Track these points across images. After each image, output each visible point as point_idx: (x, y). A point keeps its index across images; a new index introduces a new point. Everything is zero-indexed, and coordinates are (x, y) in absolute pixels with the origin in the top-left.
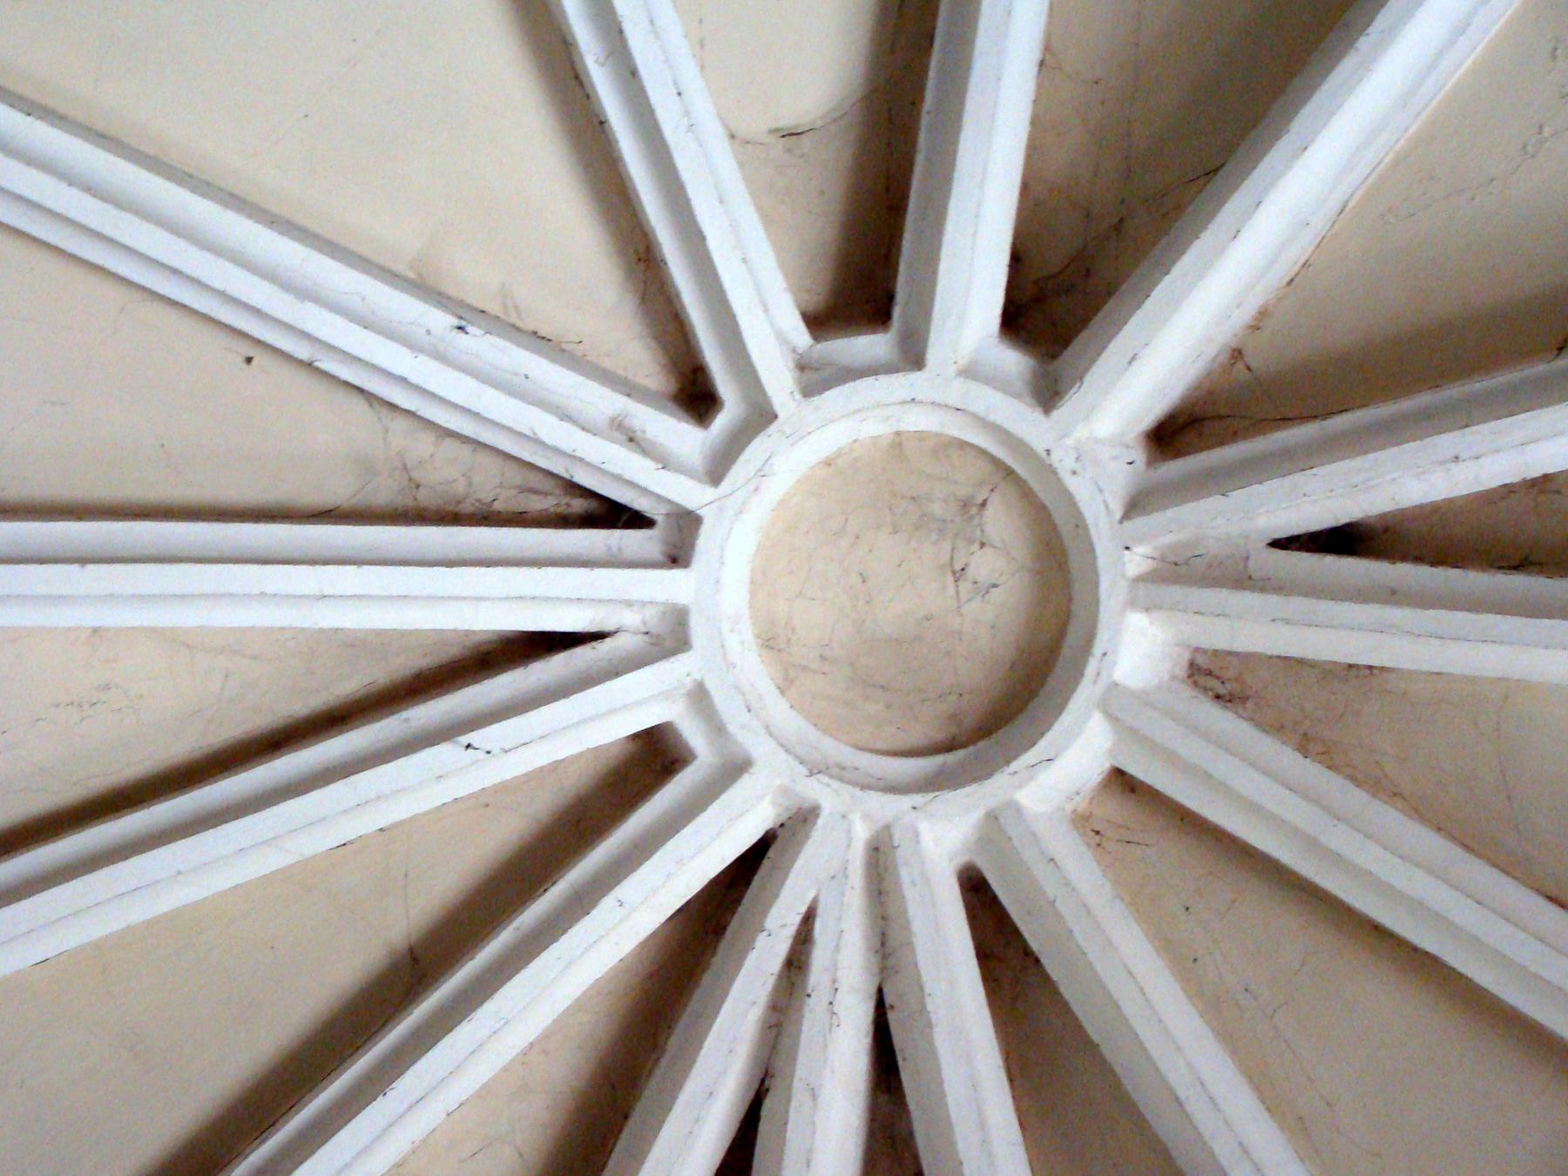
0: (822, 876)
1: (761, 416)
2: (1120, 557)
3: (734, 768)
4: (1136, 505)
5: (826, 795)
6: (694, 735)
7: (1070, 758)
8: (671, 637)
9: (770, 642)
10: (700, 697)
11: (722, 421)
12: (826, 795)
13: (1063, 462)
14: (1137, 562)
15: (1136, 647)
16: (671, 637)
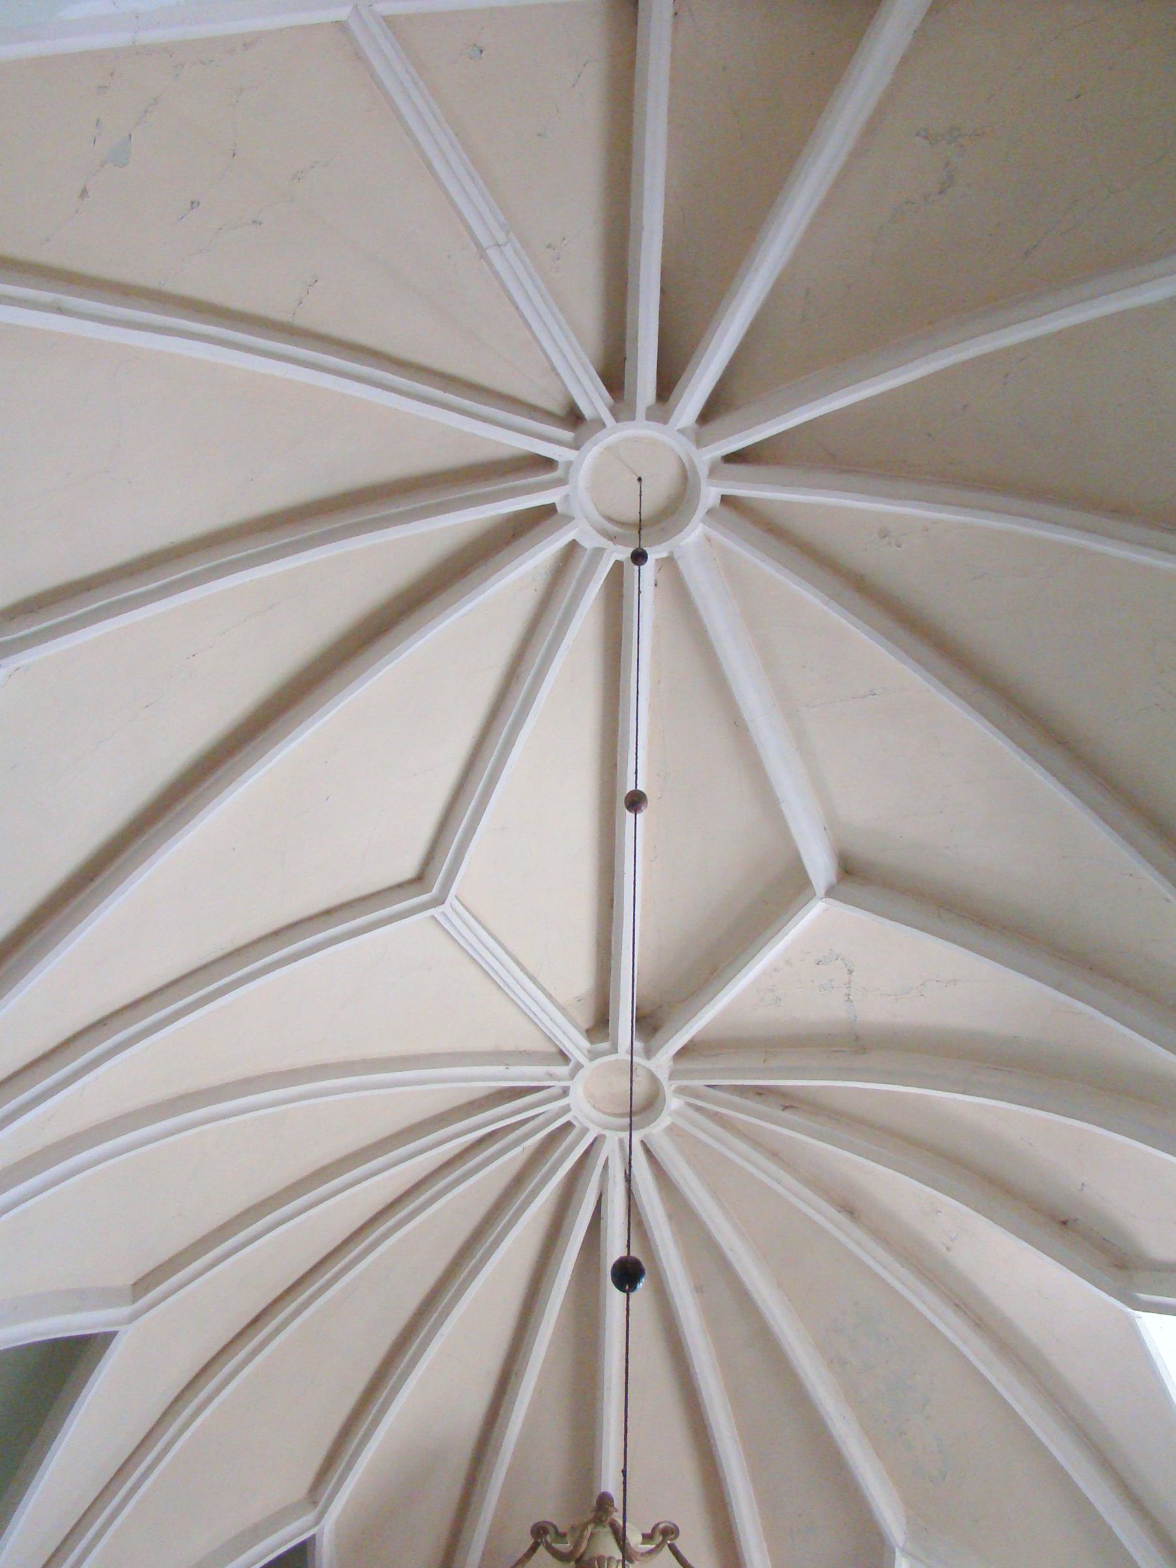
0: (611, 1150)
1: (579, 1066)
2: (668, 1087)
3: (585, 1131)
4: (672, 1076)
5: (606, 1133)
6: (575, 1123)
7: (665, 1120)
8: (567, 1109)
9: (590, 1097)
10: (575, 1117)
11: (571, 1064)
12: (606, 1133)
13: (653, 1070)
14: (672, 1088)
15: (674, 1103)
16: (567, 1109)
